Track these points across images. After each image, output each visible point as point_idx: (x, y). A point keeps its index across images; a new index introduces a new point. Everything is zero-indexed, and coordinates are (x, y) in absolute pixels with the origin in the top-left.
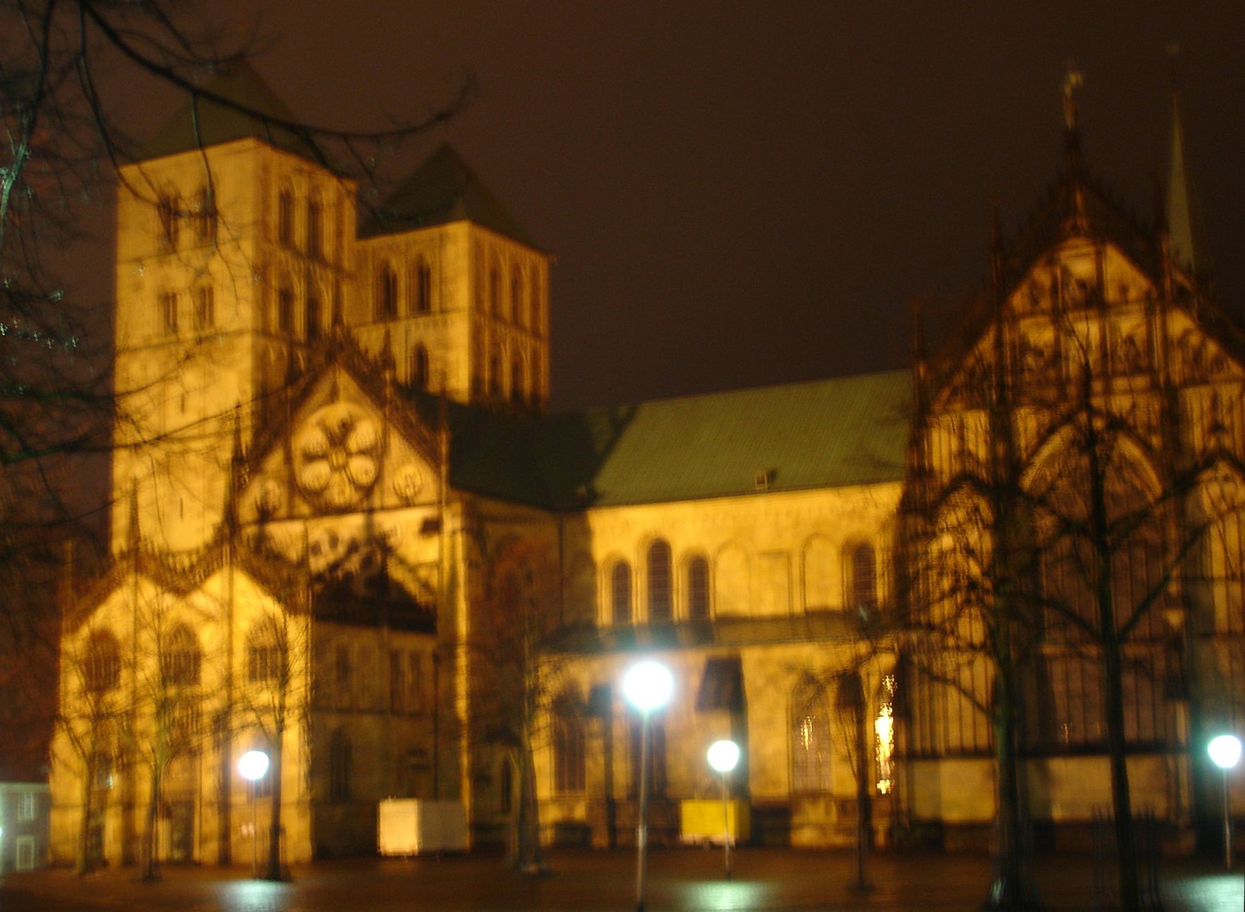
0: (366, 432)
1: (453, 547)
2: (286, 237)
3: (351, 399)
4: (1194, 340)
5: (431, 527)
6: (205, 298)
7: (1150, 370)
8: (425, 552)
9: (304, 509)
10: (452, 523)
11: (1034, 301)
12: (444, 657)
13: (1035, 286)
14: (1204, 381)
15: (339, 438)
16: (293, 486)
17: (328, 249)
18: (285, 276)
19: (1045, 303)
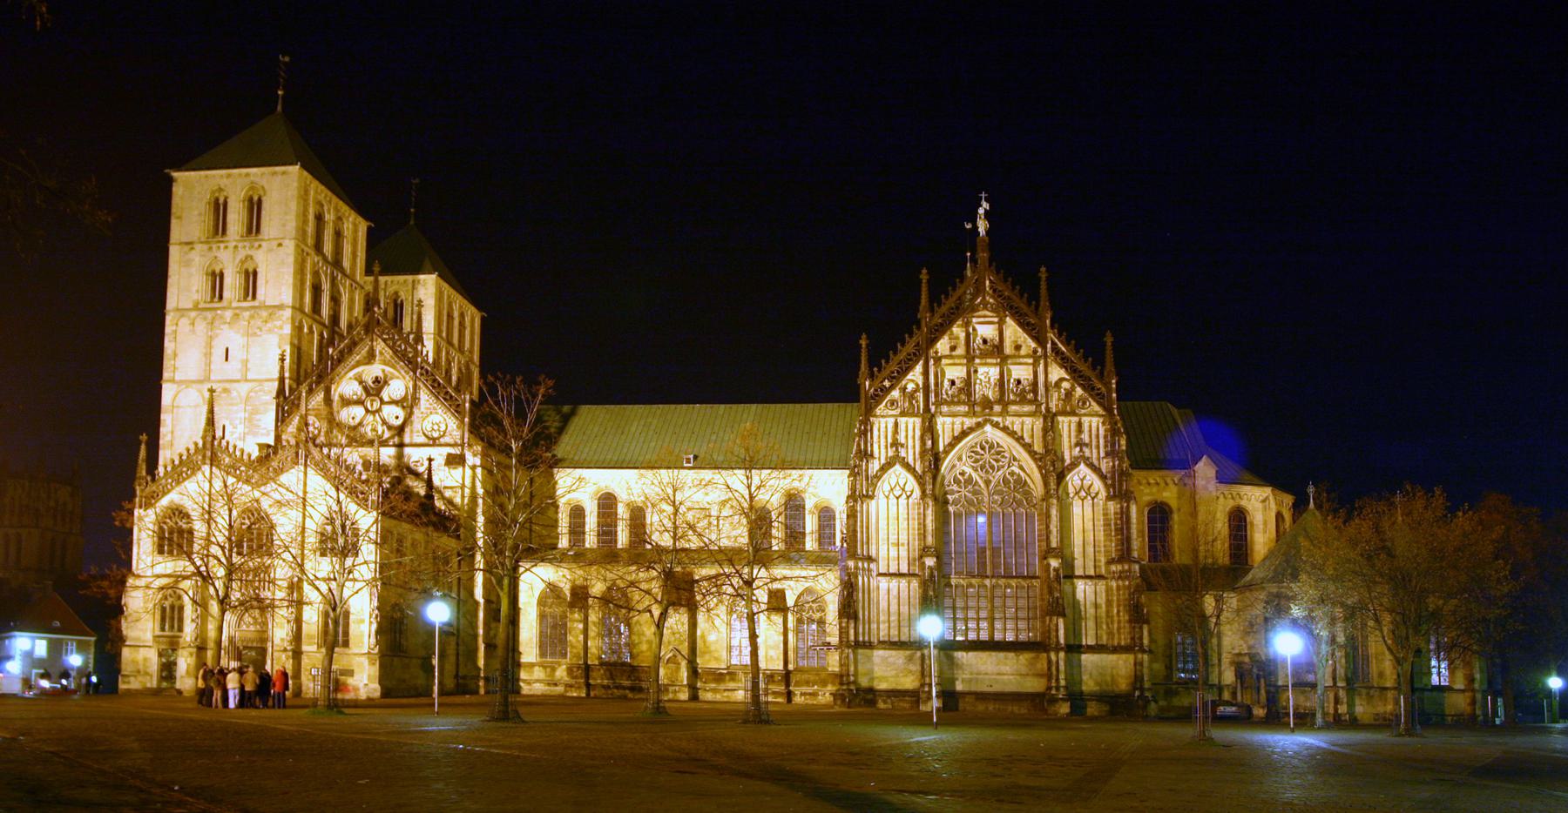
0: (398, 387)
1: (474, 477)
2: (318, 247)
3: (385, 363)
4: (1065, 385)
5: (455, 461)
7: (1035, 401)
8: (445, 477)
10: (472, 459)
11: (953, 348)
12: (468, 554)
13: (954, 338)
14: (1073, 413)
17: (346, 264)
18: (316, 274)
19: (961, 351)
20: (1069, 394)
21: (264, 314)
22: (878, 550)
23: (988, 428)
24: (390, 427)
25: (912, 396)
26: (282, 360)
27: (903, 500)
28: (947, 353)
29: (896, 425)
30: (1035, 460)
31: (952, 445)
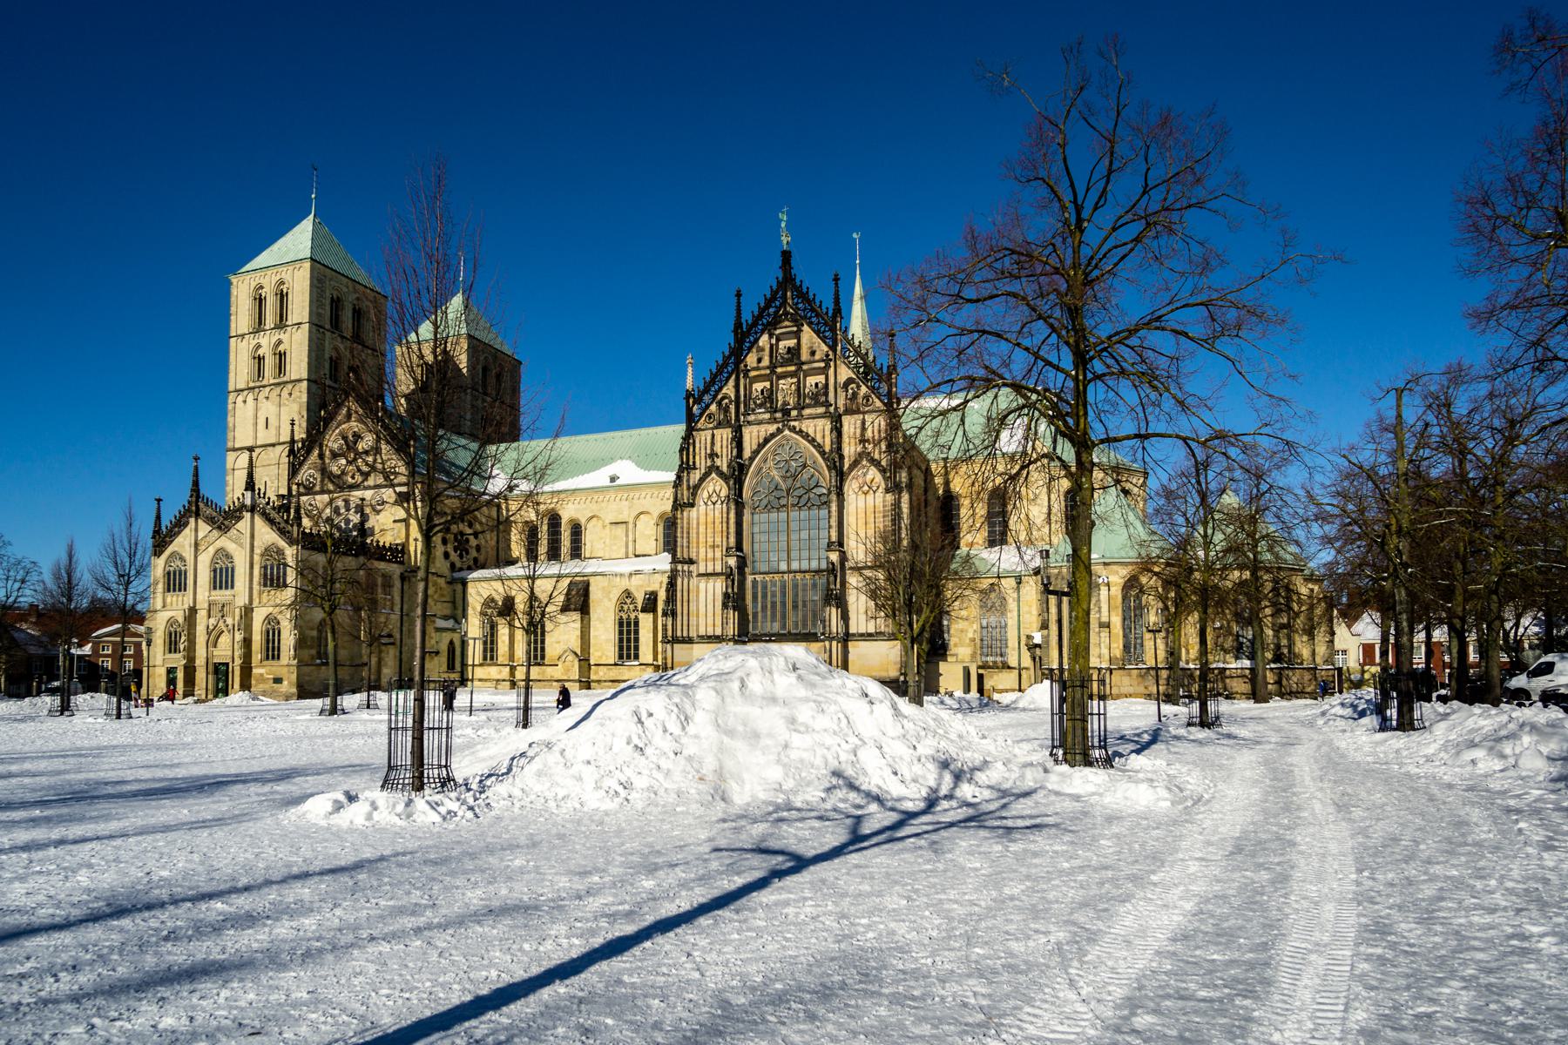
0: (367, 441)
6: (281, 357)
7: (827, 404)
9: (331, 487)
11: (759, 360)
14: (858, 412)
15: (351, 443)
16: (324, 471)
19: (766, 362)
20: (855, 395)
21: (290, 386)
22: (698, 552)
23: (787, 432)
24: (362, 473)
25: (727, 410)
26: (293, 424)
27: (718, 506)
28: (755, 365)
29: (713, 436)
30: (824, 459)
31: (755, 453)
